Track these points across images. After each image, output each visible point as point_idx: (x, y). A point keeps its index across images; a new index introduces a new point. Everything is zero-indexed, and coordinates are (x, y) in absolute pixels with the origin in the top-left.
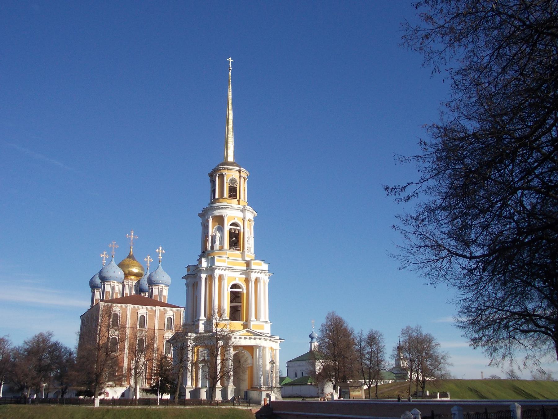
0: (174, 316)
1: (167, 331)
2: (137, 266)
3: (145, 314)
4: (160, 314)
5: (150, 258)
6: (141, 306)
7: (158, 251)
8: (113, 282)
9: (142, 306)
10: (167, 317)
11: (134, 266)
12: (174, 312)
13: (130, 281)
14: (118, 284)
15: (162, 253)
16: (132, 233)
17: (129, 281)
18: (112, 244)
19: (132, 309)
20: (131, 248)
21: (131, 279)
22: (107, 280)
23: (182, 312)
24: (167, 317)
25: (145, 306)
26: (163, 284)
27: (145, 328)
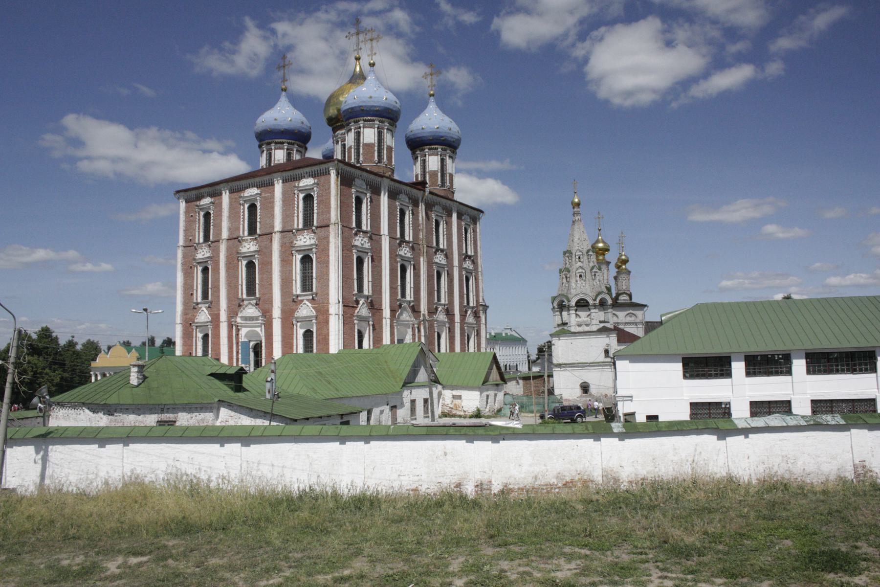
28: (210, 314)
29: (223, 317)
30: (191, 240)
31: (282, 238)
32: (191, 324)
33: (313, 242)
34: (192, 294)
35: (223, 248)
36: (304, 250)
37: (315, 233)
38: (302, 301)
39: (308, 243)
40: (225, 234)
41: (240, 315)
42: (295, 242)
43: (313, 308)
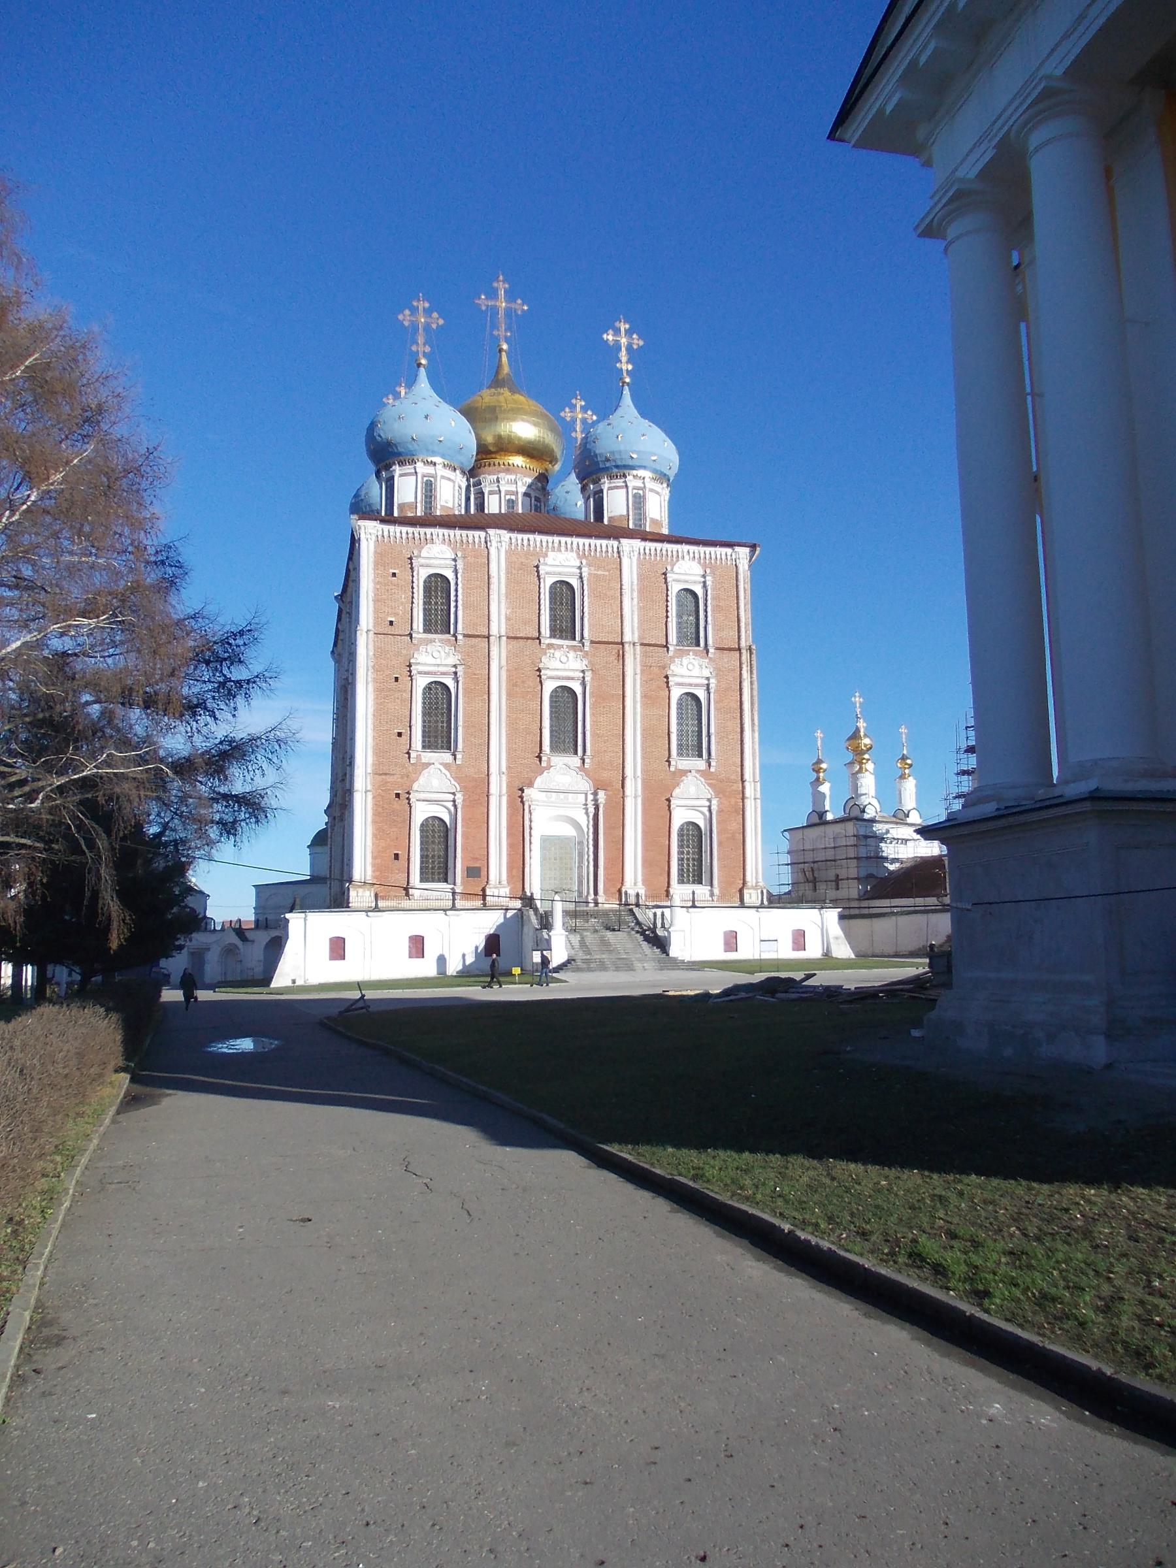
0: (709, 583)
1: (680, 654)
2: (526, 413)
3: (572, 575)
4: (642, 577)
5: (584, 409)
6: (550, 539)
7: (610, 338)
8: (427, 463)
9: (556, 539)
10: (675, 588)
11: (516, 413)
12: (704, 566)
13: (505, 477)
14: (448, 473)
15: (629, 348)
16: (502, 287)
17: (501, 475)
18: (414, 310)
19: (509, 553)
20: (501, 350)
21: (510, 469)
22: (400, 454)
23: (744, 565)
24: (675, 588)
25: (569, 540)
26: (644, 468)
27: (578, 637)
28: (456, 779)
29: (498, 787)
30: (391, 623)
31: (645, 655)
32: (398, 795)
33: (706, 673)
34: (400, 734)
35: (499, 654)
36: (691, 685)
37: (710, 659)
38: (685, 772)
39: (696, 672)
40: (498, 627)
41: (536, 785)
42: (672, 667)
43: (709, 784)
